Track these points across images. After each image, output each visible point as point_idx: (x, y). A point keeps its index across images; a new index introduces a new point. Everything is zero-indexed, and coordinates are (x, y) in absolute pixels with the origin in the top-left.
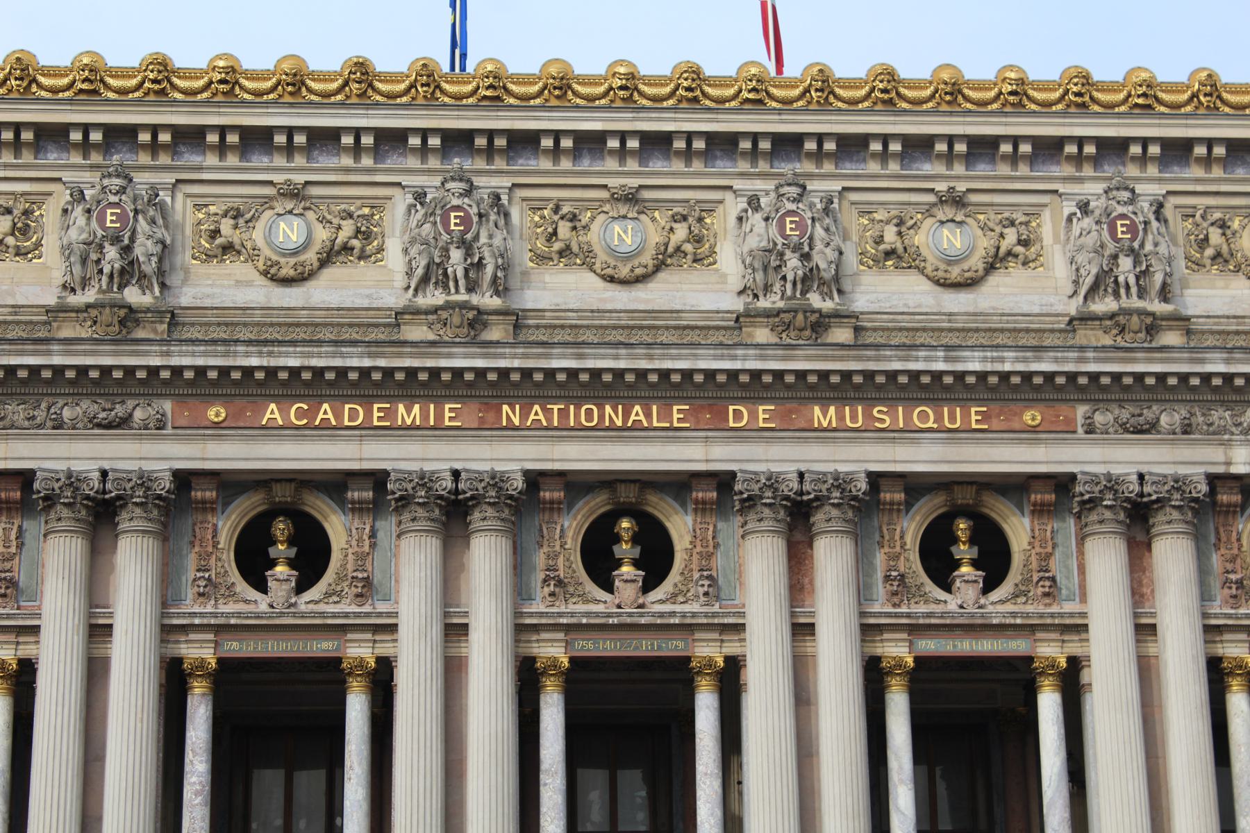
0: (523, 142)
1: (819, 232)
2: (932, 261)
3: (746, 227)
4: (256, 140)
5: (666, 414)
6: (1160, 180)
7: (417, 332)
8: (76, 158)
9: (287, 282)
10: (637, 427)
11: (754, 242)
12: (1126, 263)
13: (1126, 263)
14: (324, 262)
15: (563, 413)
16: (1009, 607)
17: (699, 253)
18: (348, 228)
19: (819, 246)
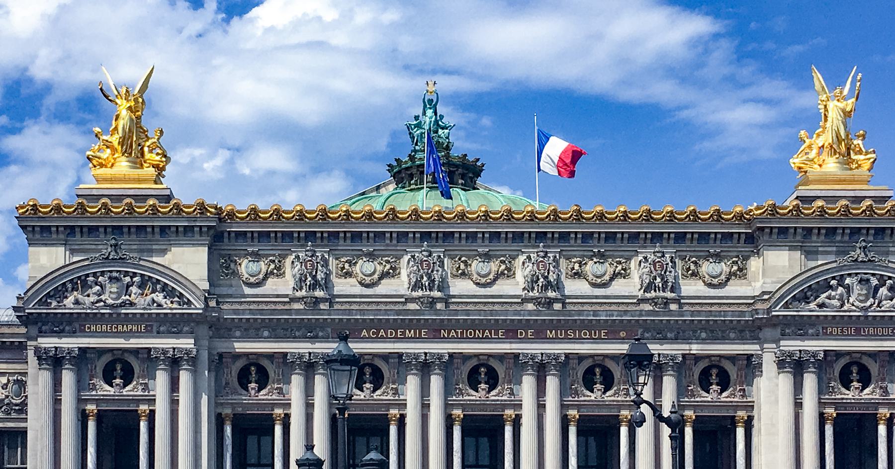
0: (448, 236)
1: (552, 268)
2: (590, 277)
3: (526, 265)
4: (356, 237)
5: (497, 333)
6: (674, 247)
7: (412, 306)
8: (296, 243)
9: (367, 286)
10: (487, 337)
11: (527, 272)
12: (658, 280)
13: (658, 280)
14: (380, 278)
15: (462, 333)
16: (612, 398)
17: (509, 273)
18: (388, 266)
19: (551, 273)
